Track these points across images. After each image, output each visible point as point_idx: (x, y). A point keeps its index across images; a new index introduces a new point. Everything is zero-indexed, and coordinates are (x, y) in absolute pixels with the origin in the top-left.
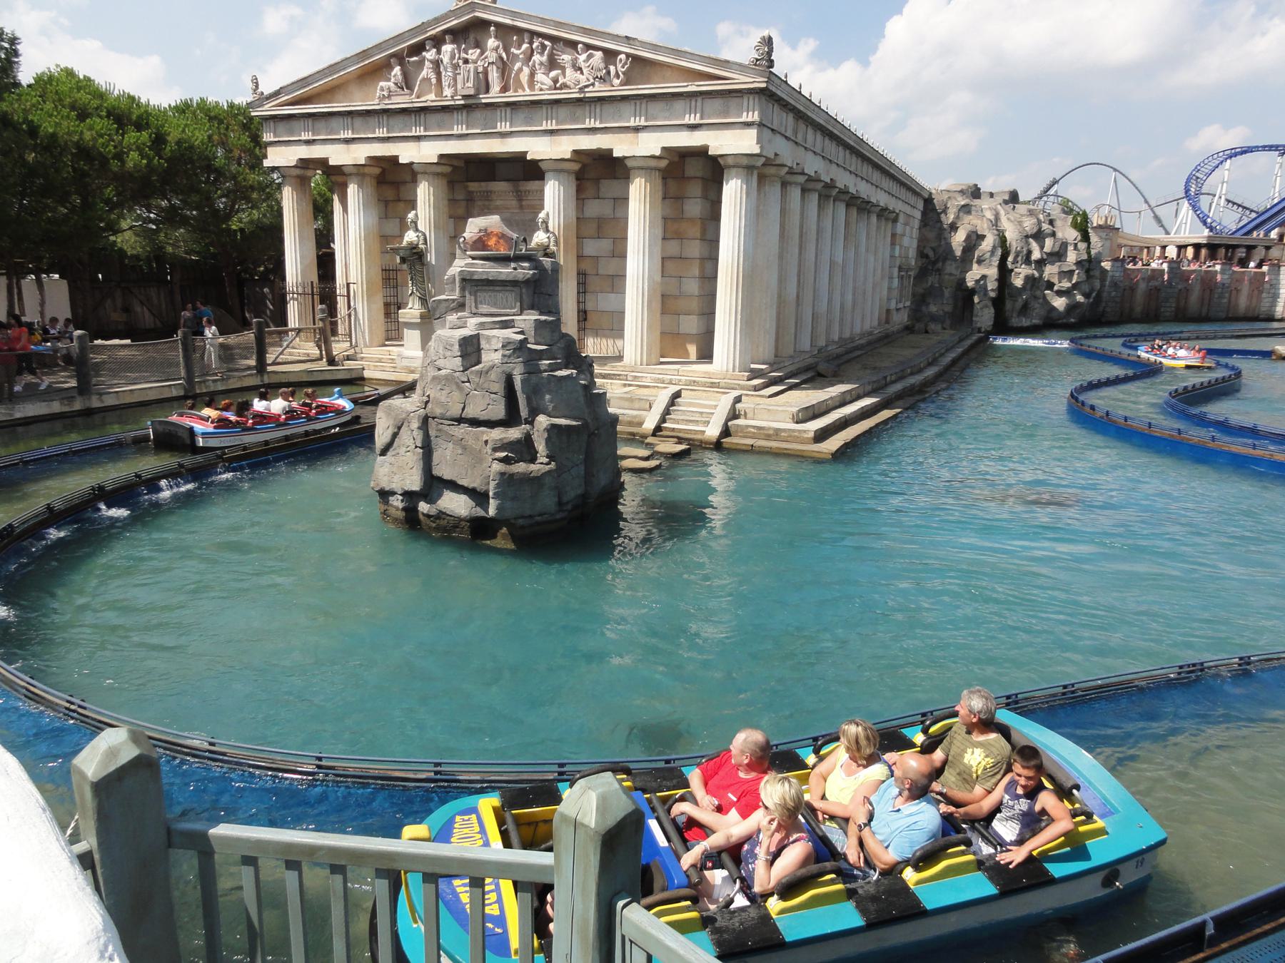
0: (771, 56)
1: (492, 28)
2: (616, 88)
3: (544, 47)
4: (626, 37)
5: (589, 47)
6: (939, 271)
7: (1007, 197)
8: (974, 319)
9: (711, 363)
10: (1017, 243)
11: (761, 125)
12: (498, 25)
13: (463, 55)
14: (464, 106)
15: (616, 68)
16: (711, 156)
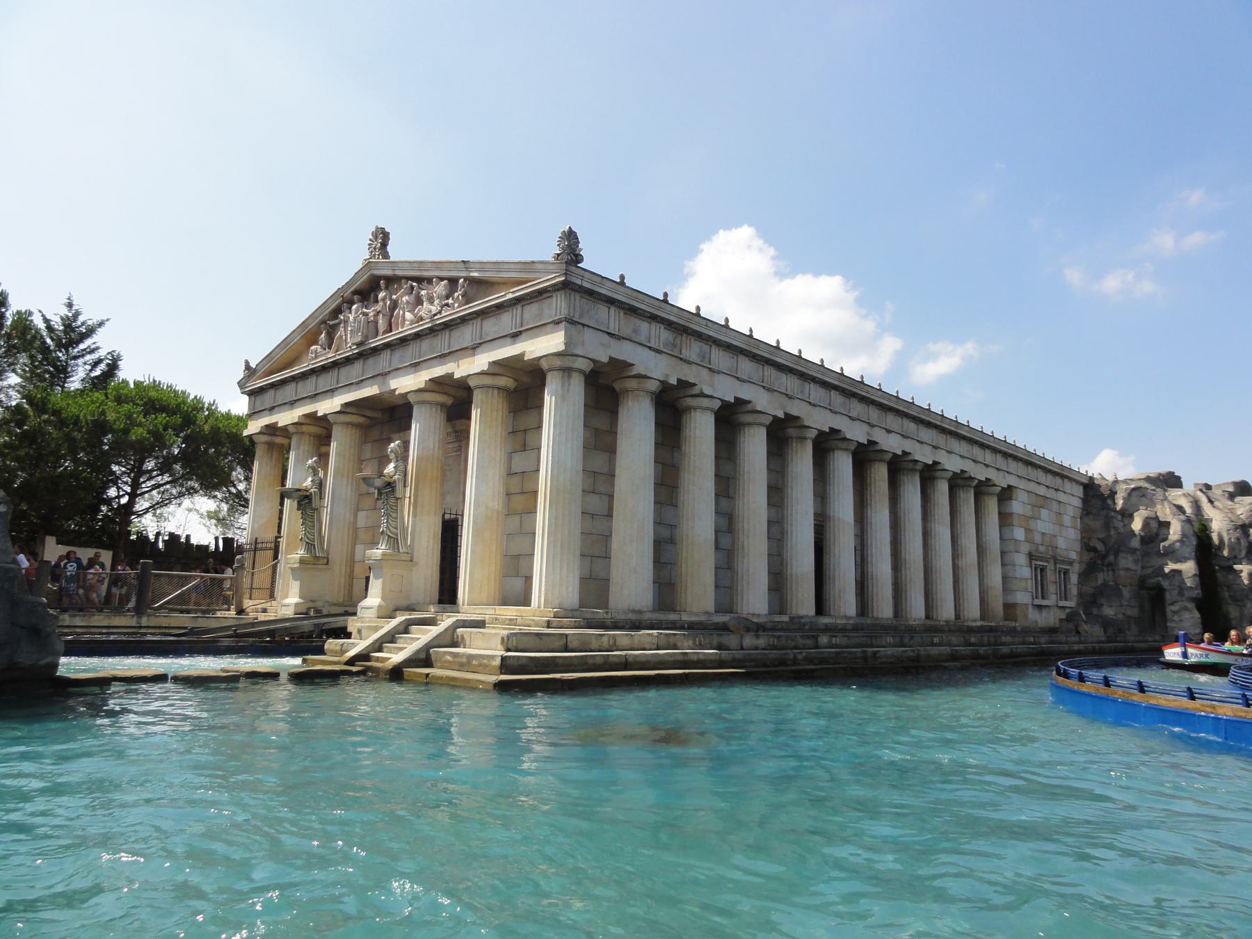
2: (457, 310)
3: (412, 287)
4: (463, 262)
5: (442, 279)
6: (1112, 567)
7: (1231, 489)
8: (1169, 624)
10: (1228, 534)
13: (365, 310)
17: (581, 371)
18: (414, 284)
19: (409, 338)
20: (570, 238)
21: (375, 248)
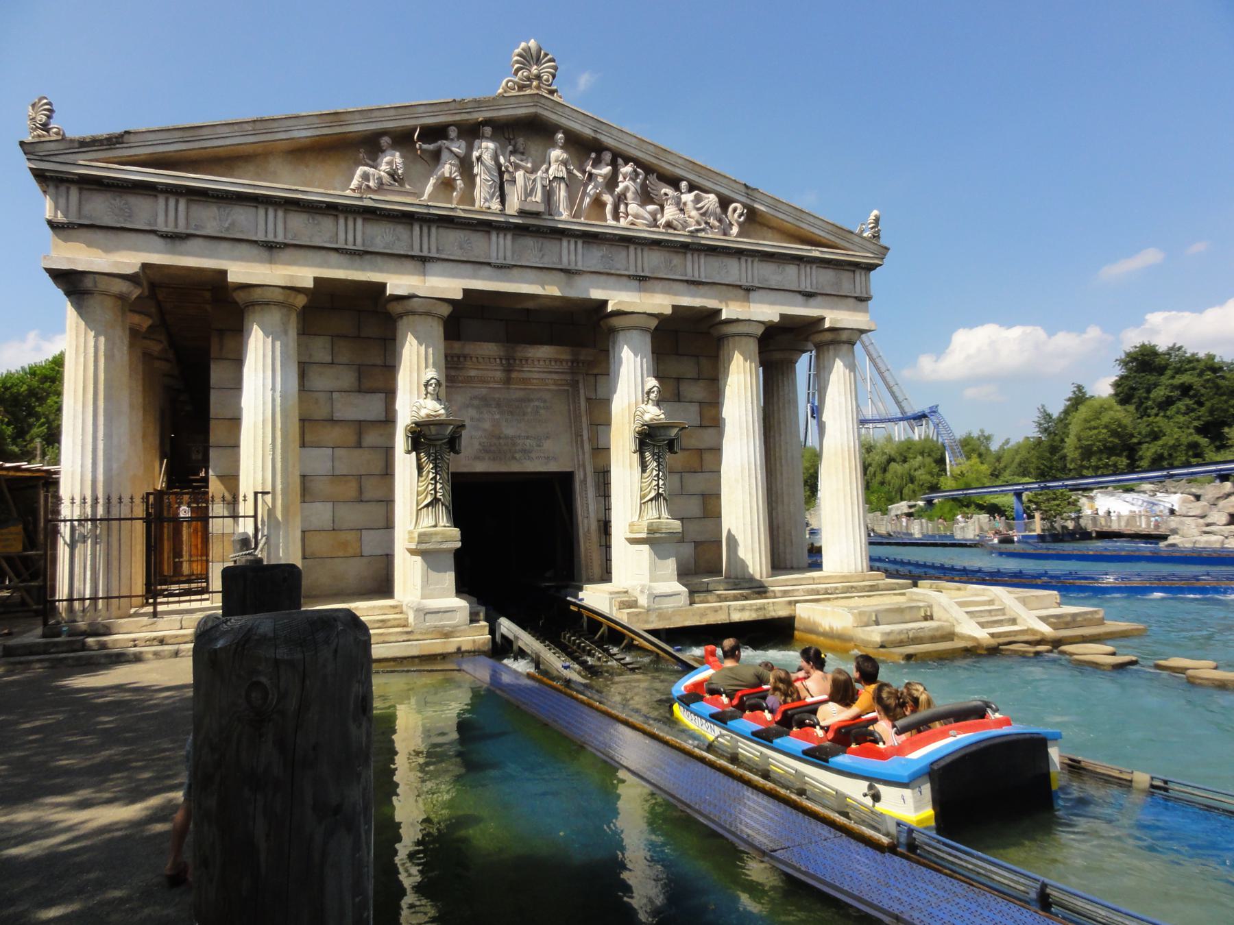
1: (560, 135)
3: (637, 174)
4: (745, 185)
9: (822, 570)
14: (517, 226)
15: (727, 217)
18: (639, 170)
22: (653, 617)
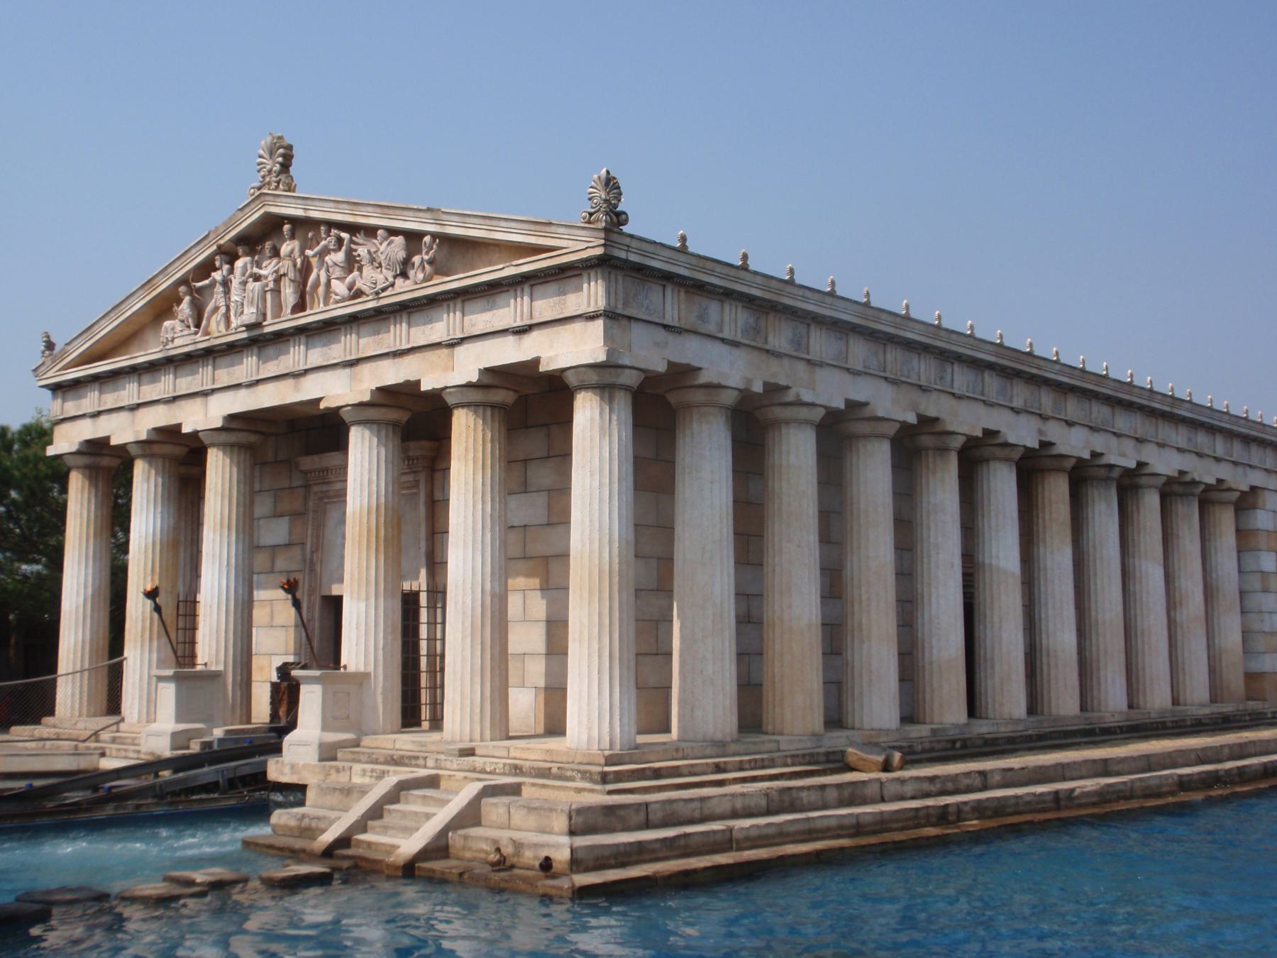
0: (616, 206)
1: (287, 227)
3: (340, 241)
5: (393, 232)
11: (610, 315)
12: (294, 221)
13: (256, 270)
16: (541, 372)
17: (626, 388)
19: (338, 321)
20: (610, 183)
21: (270, 171)
22: (287, 770)
